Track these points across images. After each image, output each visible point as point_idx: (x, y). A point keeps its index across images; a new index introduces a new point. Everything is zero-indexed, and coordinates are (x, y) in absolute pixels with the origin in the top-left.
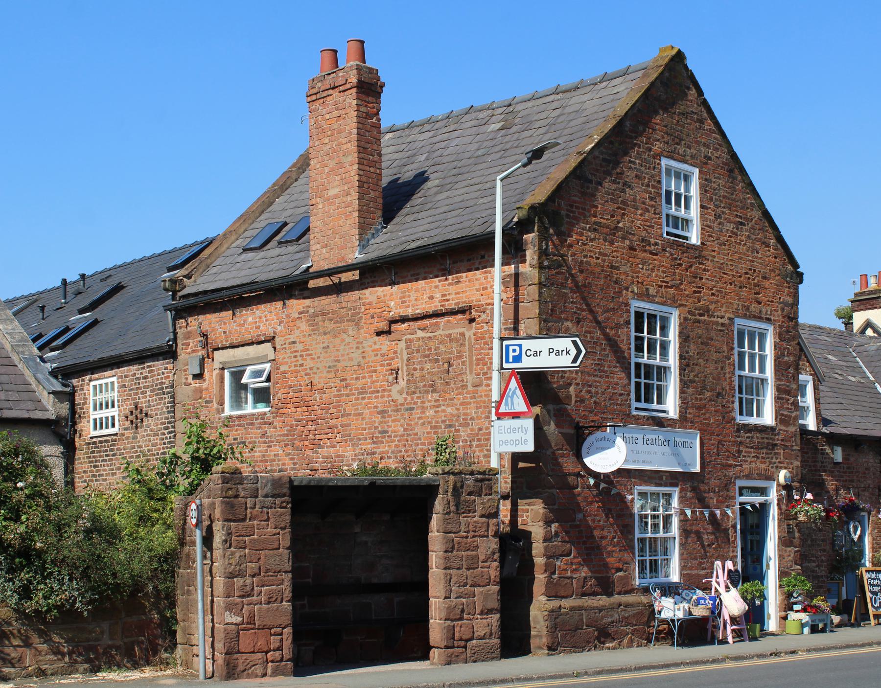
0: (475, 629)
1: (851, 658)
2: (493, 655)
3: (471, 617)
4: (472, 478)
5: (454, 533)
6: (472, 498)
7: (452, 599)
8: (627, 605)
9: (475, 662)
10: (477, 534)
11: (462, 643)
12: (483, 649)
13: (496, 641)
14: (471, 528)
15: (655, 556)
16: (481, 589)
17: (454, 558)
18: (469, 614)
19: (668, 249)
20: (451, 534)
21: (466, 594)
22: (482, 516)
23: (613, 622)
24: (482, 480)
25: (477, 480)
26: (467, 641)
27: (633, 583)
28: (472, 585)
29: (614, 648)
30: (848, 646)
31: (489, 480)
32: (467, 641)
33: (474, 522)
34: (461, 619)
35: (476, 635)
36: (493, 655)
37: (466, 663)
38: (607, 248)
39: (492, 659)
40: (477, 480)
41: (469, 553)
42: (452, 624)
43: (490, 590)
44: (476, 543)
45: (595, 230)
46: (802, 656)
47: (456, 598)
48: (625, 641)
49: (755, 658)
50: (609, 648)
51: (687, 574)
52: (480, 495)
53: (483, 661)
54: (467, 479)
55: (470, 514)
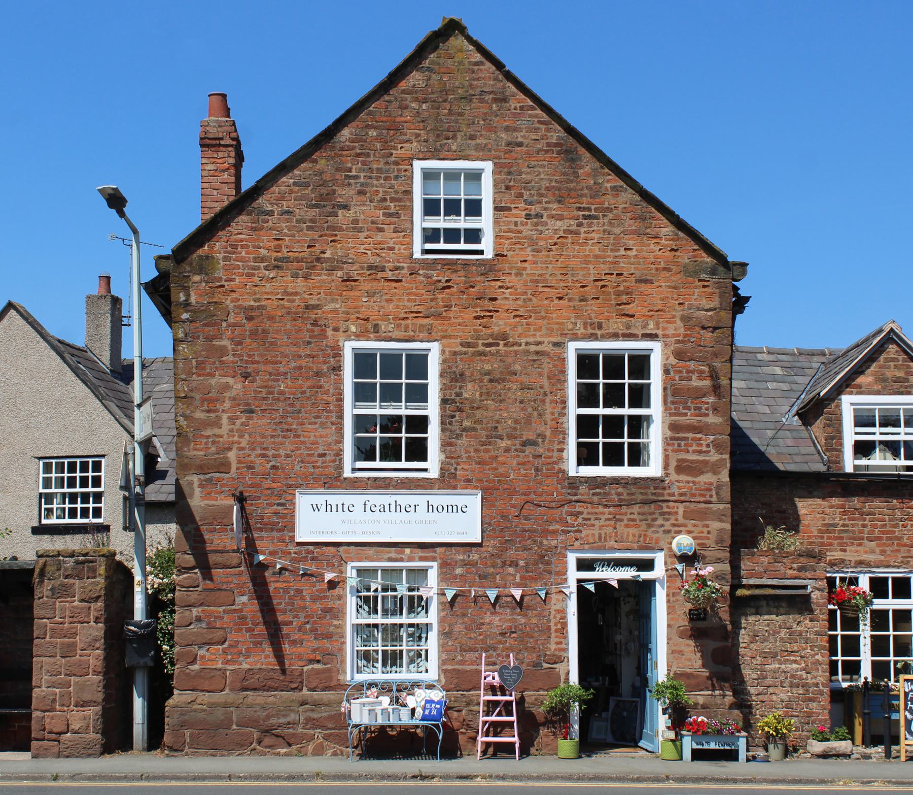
0: (70, 722)
1: (99, 789)
2: (90, 751)
3: (66, 708)
4: (72, 560)
5: (48, 619)
6: (72, 581)
7: (44, 689)
8: (317, 704)
9: (67, 757)
10: (75, 619)
11: (54, 736)
12: (78, 744)
13: (94, 737)
14: (68, 613)
15: (400, 646)
16: (78, 679)
17: (47, 646)
18: (63, 705)
19: (421, 272)
20: (44, 620)
21: (60, 684)
22: (82, 600)
23: (289, 723)
24: (83, 562)
25: (78, 563)
26: (60, 733)
27: (341, 677)
28: (66, 675)
29: (286, 754)
30: (799, 782)
31: (92, 562)
32: (60, 733)
33: (73, 607)
34: (53, 710)
35: (71, 727)
36: (90, 751)
37: (59, 757)
38: (300, 285)
39: (89, 755)
40: (78, 563)
41: (66, 640)
42: (42, 715)
43: (89, 681)
44: (74, 630)
45: (277, 267)
46: (479, 782)
47: (48, 687)
48: (311, 747)
49: (479, 779)
50: (279, 754)
51: (454, 670)
52: (80, 579)
53: (77, 757)
54: (64, 562)
55: (69, 599)
